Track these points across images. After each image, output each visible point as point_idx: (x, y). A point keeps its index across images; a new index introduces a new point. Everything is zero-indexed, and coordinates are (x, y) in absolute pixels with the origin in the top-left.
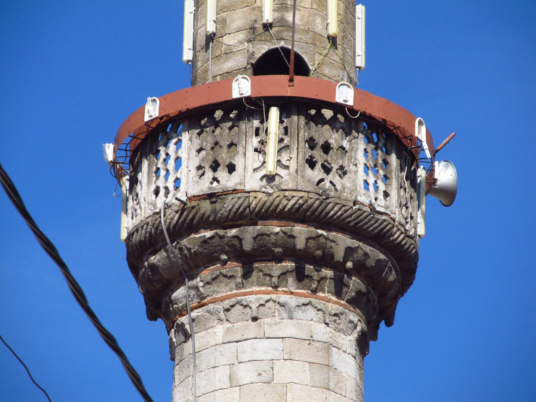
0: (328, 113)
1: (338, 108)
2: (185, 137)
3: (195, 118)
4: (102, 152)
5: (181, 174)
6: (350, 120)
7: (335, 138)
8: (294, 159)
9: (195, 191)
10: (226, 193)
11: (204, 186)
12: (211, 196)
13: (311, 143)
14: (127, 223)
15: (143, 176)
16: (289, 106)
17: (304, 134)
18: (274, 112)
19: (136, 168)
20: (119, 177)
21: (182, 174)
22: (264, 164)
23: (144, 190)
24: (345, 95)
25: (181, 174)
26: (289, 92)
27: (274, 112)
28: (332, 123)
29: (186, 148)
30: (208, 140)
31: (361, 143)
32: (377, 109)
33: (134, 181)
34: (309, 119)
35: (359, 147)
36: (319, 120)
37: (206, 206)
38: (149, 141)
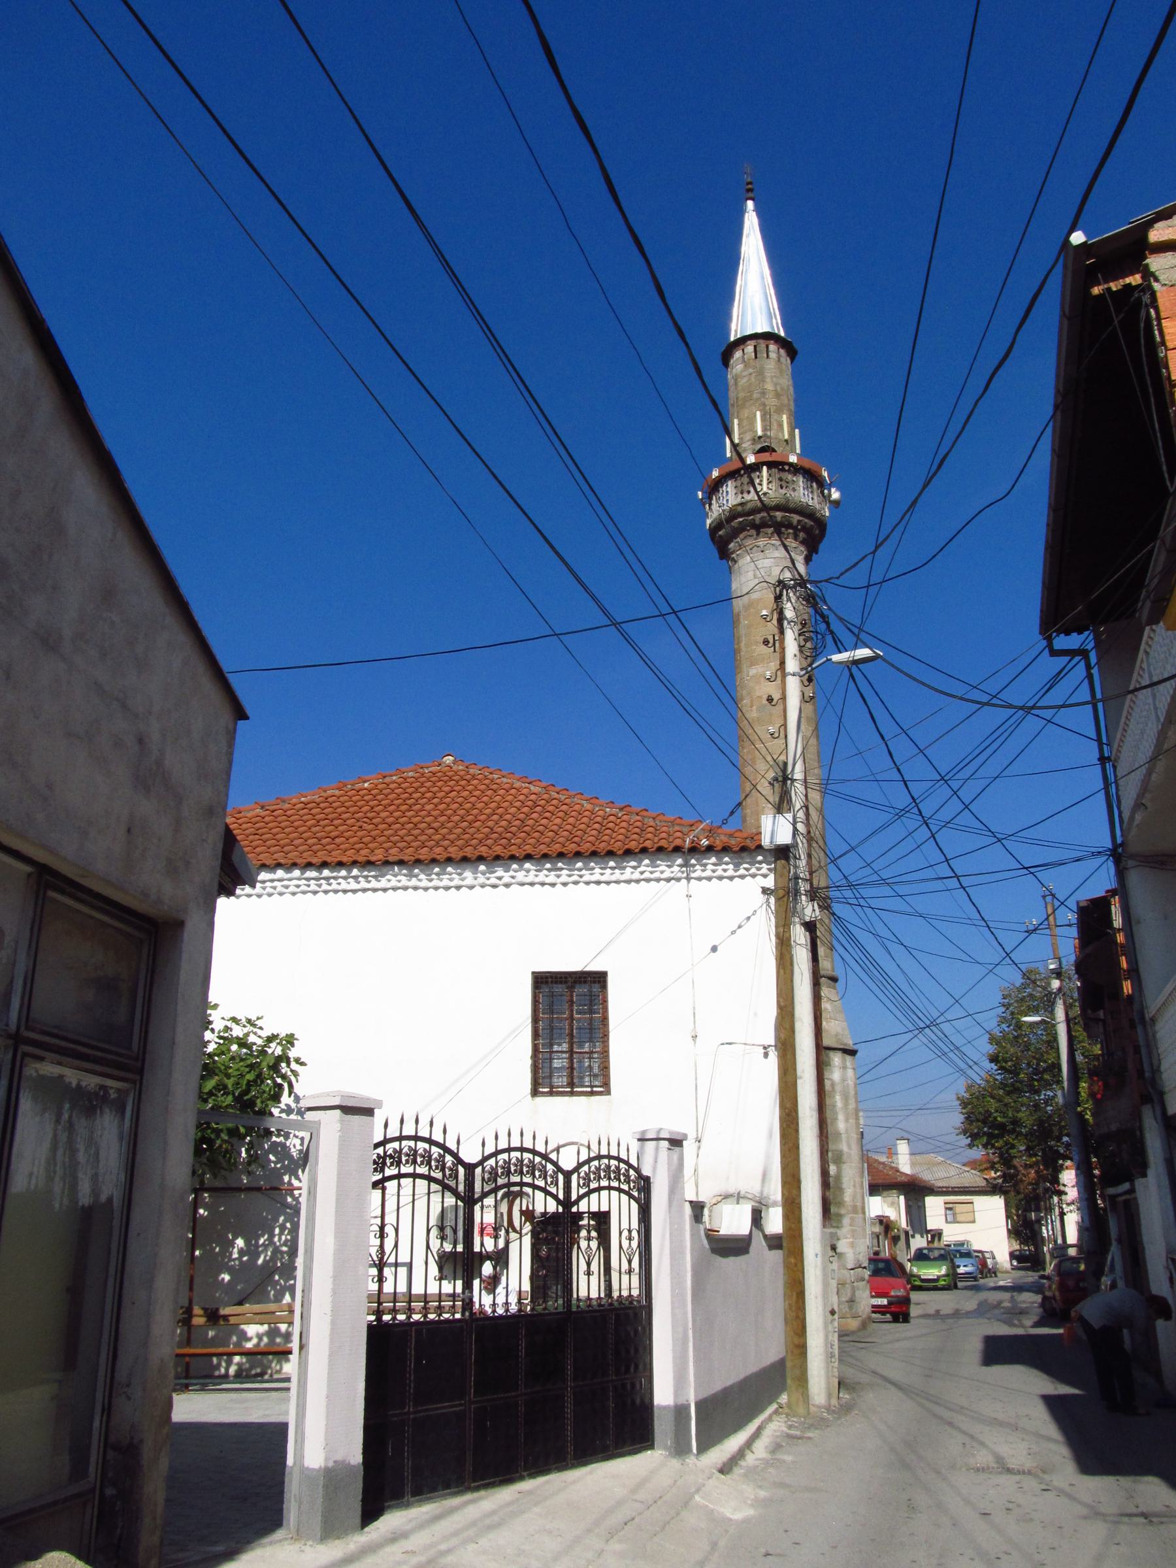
0: (787, 468)
1: (791, 465)
2: (729, 483)
3: (732, 475)
4: (697, 495)
5: (730, 496)
6: (796, 469)
7: (790, 477)
8: (773, 486)
9: (735, 503)
10: (747, 502)
11: (739, 500)
12: (741, 504)
13: (781, 479)
14: (708, 522)
15: (714, 502)
16: (771, 465)
17: (778, 476)
18: (765, 468)
19: (710, 499)
20: (704, 505)
21: (729, 497)
22: (766, 485)
23: (715, 506)
24: (793, 459)
25: (730, 496)
26: (770, 459)
27: (765, 468)
28: (789, 471)
29: (730, 487)
30: (739, 483)
31: (801, 479)
32: (807, 464)
33: (710, 505)
34: (780, 470)
35: (800, 481)
36: (783, 470)
37: (740, 508)
38: (714, 488)
